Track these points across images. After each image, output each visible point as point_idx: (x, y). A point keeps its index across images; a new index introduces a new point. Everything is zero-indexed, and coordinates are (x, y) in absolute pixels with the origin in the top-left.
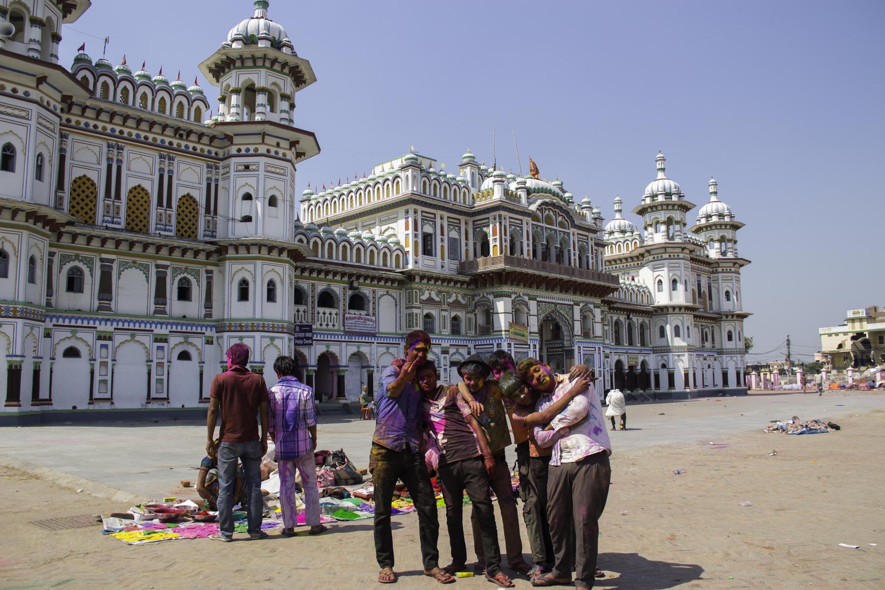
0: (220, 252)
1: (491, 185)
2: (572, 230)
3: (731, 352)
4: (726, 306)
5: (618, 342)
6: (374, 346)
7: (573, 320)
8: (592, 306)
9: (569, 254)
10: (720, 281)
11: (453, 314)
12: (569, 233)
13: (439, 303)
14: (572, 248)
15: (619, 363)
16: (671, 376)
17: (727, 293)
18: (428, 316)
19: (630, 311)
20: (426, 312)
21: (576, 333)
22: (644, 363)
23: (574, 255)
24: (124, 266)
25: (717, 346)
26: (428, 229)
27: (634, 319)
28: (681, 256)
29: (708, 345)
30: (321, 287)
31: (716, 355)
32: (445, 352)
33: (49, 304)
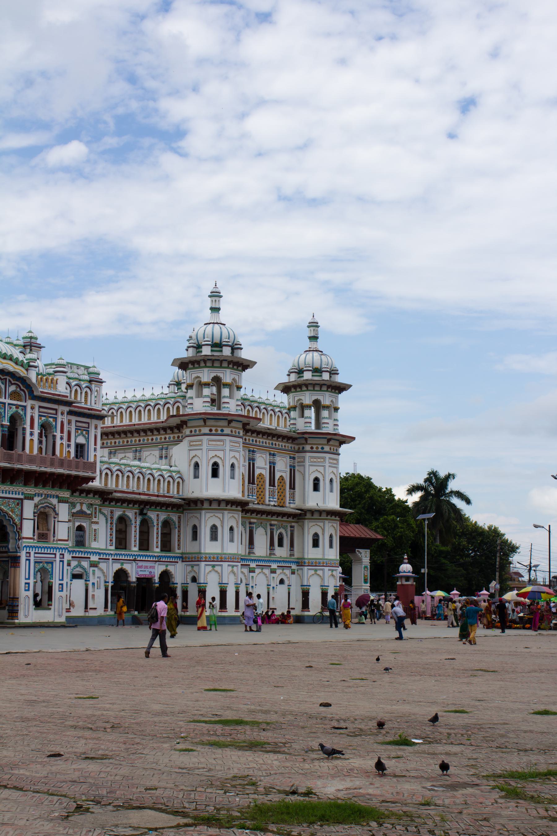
3: (316, 564)
5: (121, 542)
7: (22, 519)
8: (54, 501)
9: (24, 434)
10: (307, 463)
12: (25, 407)
14: (28, 426)
15: (121, 575)
16: (202, 593)
17: (316, 480)
19: (144, 505)
22: (165, 576)
23: (32, 434)
25: (297, 555)
27: (152, 515)
28: (227, 431)
29: (281, 552)
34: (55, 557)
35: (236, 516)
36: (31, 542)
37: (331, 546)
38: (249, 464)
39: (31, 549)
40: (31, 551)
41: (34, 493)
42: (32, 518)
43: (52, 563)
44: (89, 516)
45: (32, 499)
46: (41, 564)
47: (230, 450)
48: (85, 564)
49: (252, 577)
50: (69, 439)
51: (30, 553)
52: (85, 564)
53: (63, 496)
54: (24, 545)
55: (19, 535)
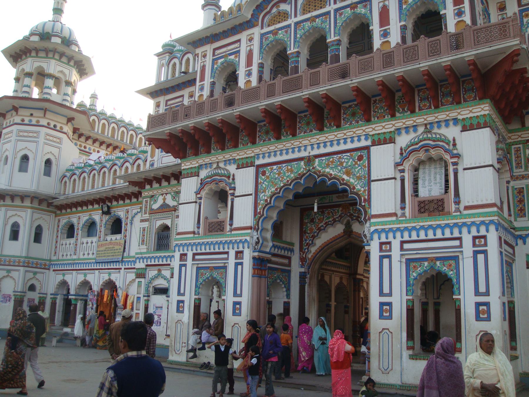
6: (122, 271)
7: (370, 181)
8: (452, 132)
18: (166, 228)
20: (159, 223)
21: (376, 208)
23: (385, 34)
30: (84, 218)
34: (461, 246)
36: (390, 223)
39: (391, 235)
40: (391, 238)
41: (392, 129)
42: (398, 176)
43: (456, 259)
45: (388, 139)
46: (426, 264)
51: (389, 243)
53: (471, 115)
54: (372, 229)
55: (366, 212)
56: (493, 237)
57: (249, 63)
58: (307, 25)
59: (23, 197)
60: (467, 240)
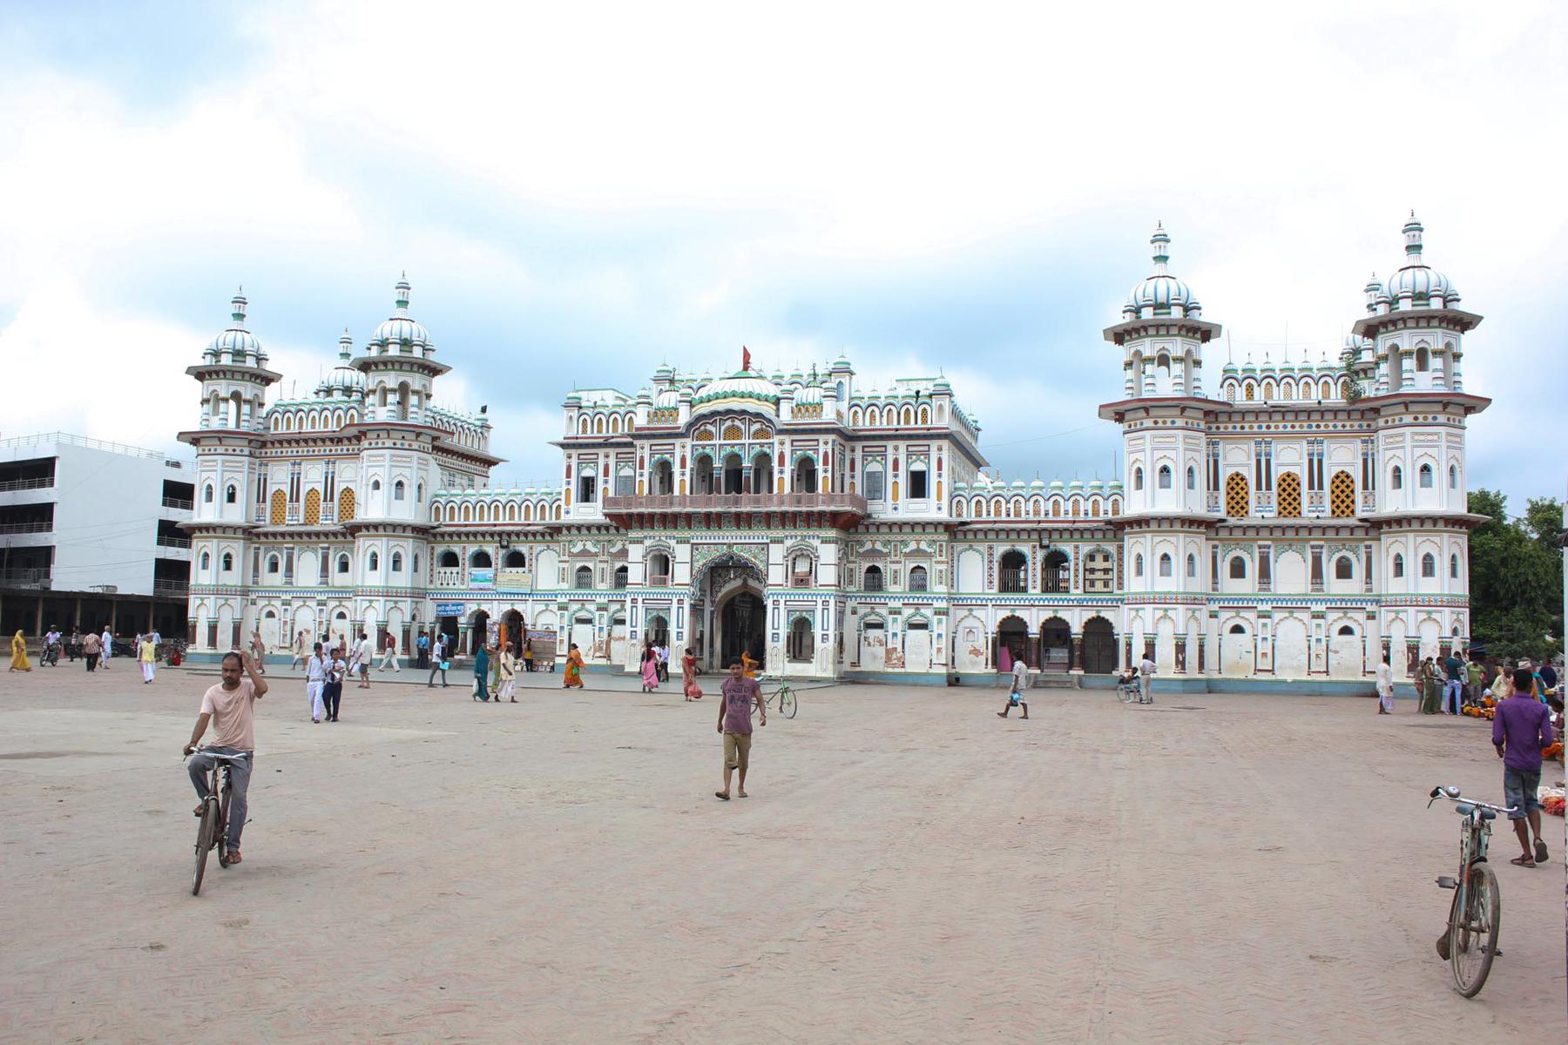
0: (353, 530)
1: (673, 404)
2: (776, 439)
3: (1399, 604)
4: (1390, 503)
8: (816, 542)
11: (618, 565)
13: (596, 555)
17: (1397, 470)
18: (585, 569)
19: (1041, 534)
20: (578, 565)
23: (781, 472)
24: (302, 551)
26: (588, 472)
27: (1067, 548)
28: (1148, 423)
31: (1369, 608)
32: (602, 608)
33: (256, 583)
35: (1173, 539)
37: (1454, 574)
38: (1259, 462)
44: (930, 556)
47: (1154, 449)
48: (928, 612)
49: (1264, 625)
50: (896, 467)
52: (928, 612)
56: (832, 602)
57: (683, 465)
58: (729, 449)
59: (404, 527)
60: (820, 602)
